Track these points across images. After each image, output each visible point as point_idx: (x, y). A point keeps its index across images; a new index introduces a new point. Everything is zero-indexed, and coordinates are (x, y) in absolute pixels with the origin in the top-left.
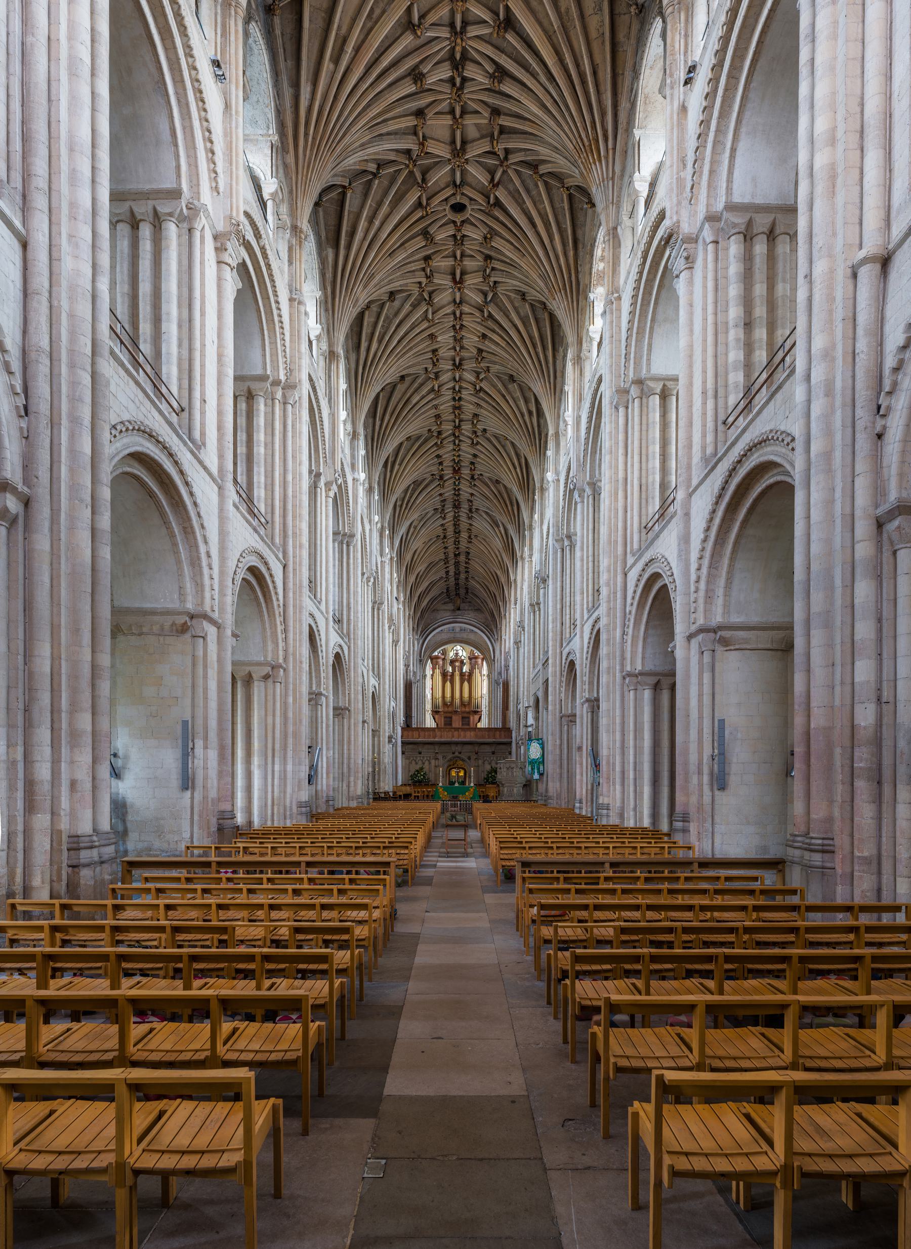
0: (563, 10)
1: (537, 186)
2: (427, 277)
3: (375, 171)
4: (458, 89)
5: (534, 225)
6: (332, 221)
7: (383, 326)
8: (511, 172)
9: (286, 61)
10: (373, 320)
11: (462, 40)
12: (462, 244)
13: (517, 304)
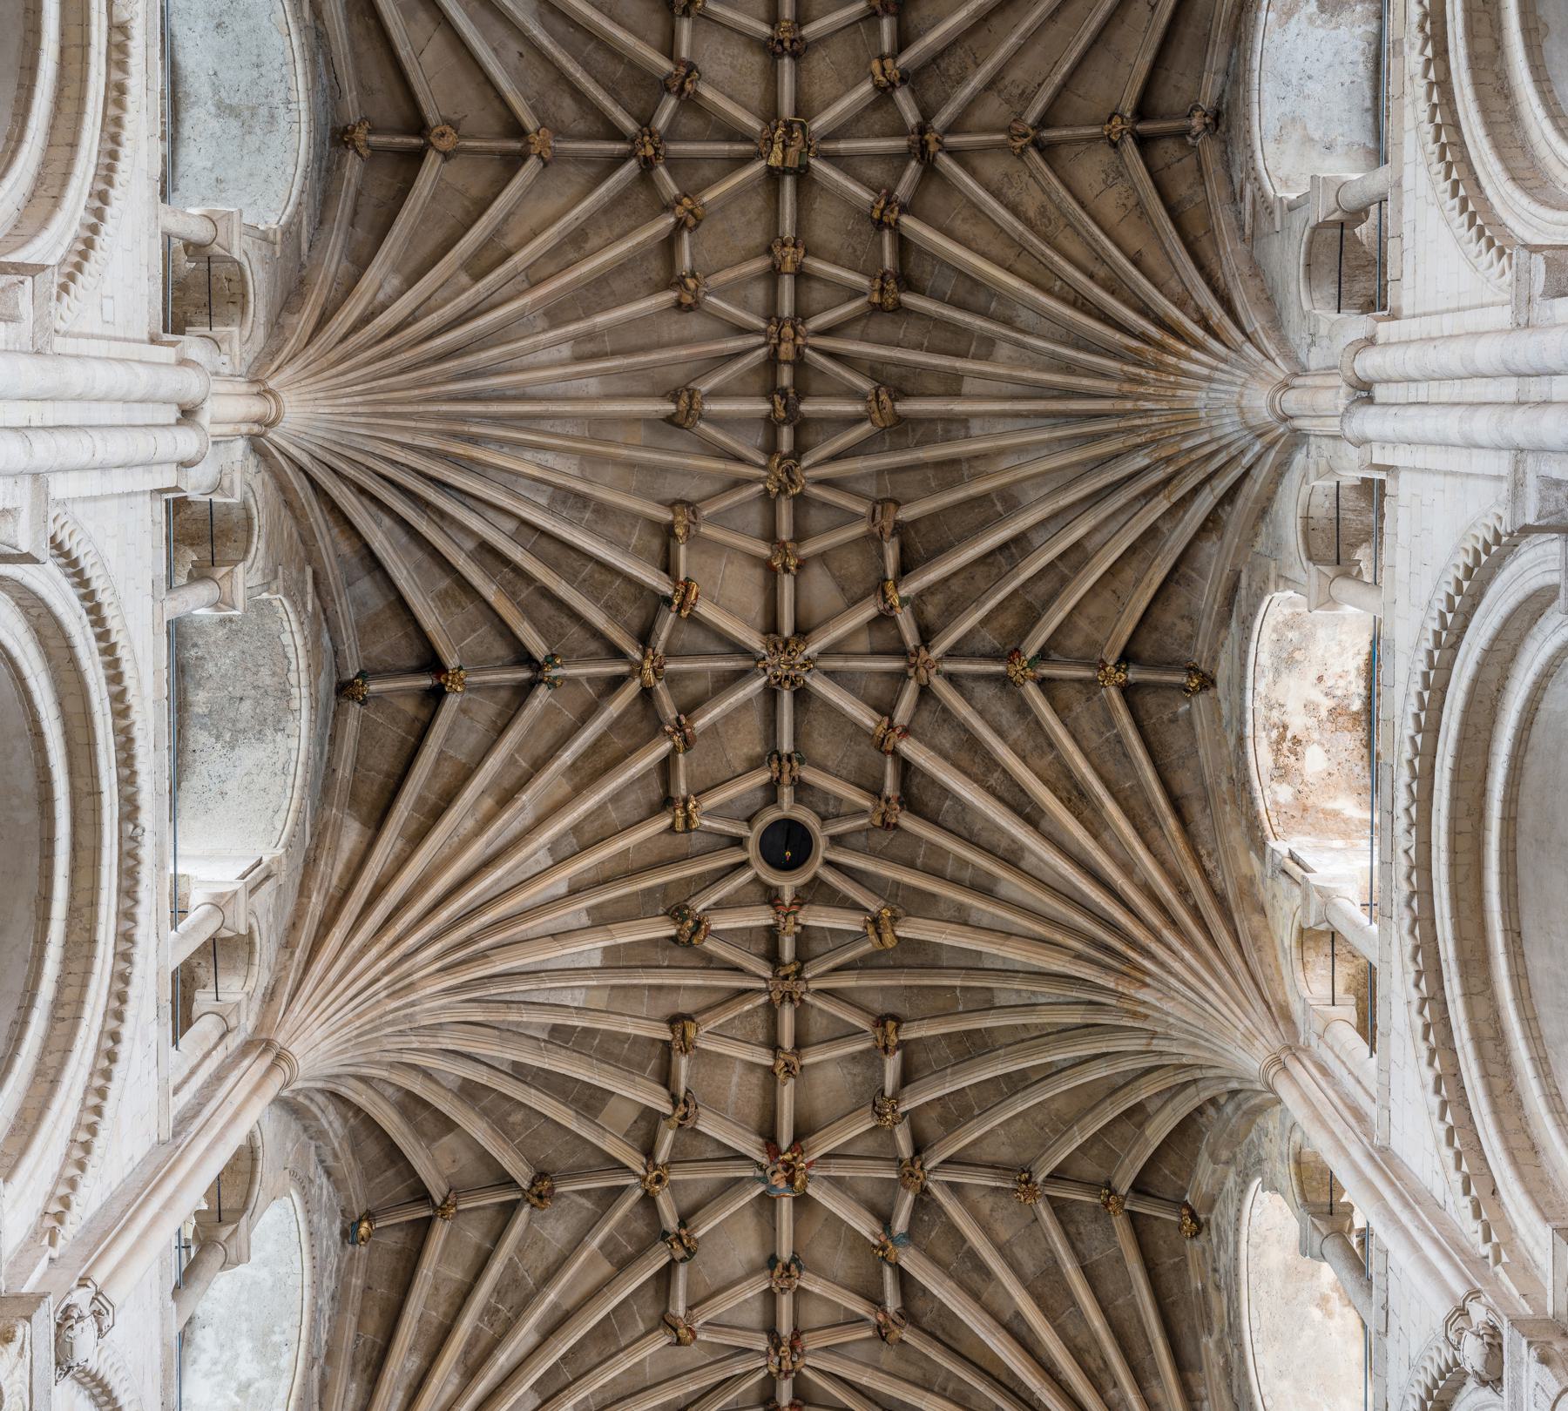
0: (1031, 214)
1: (1023, 709)
2: (674, 1100)
3: (540, 657)
4: (784, 458)
5: (1031, 815)
6: (383, 761)
7: (489, 1311)
8: (941, 687)
9: (352, 225)
10: (457, 1274)
11: (796, 333)
12: (798, 974)
13: (1004, 1234)
